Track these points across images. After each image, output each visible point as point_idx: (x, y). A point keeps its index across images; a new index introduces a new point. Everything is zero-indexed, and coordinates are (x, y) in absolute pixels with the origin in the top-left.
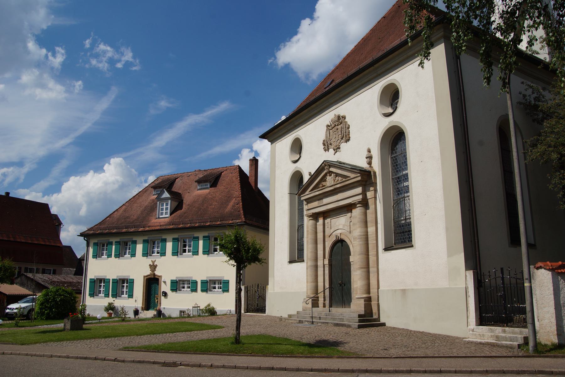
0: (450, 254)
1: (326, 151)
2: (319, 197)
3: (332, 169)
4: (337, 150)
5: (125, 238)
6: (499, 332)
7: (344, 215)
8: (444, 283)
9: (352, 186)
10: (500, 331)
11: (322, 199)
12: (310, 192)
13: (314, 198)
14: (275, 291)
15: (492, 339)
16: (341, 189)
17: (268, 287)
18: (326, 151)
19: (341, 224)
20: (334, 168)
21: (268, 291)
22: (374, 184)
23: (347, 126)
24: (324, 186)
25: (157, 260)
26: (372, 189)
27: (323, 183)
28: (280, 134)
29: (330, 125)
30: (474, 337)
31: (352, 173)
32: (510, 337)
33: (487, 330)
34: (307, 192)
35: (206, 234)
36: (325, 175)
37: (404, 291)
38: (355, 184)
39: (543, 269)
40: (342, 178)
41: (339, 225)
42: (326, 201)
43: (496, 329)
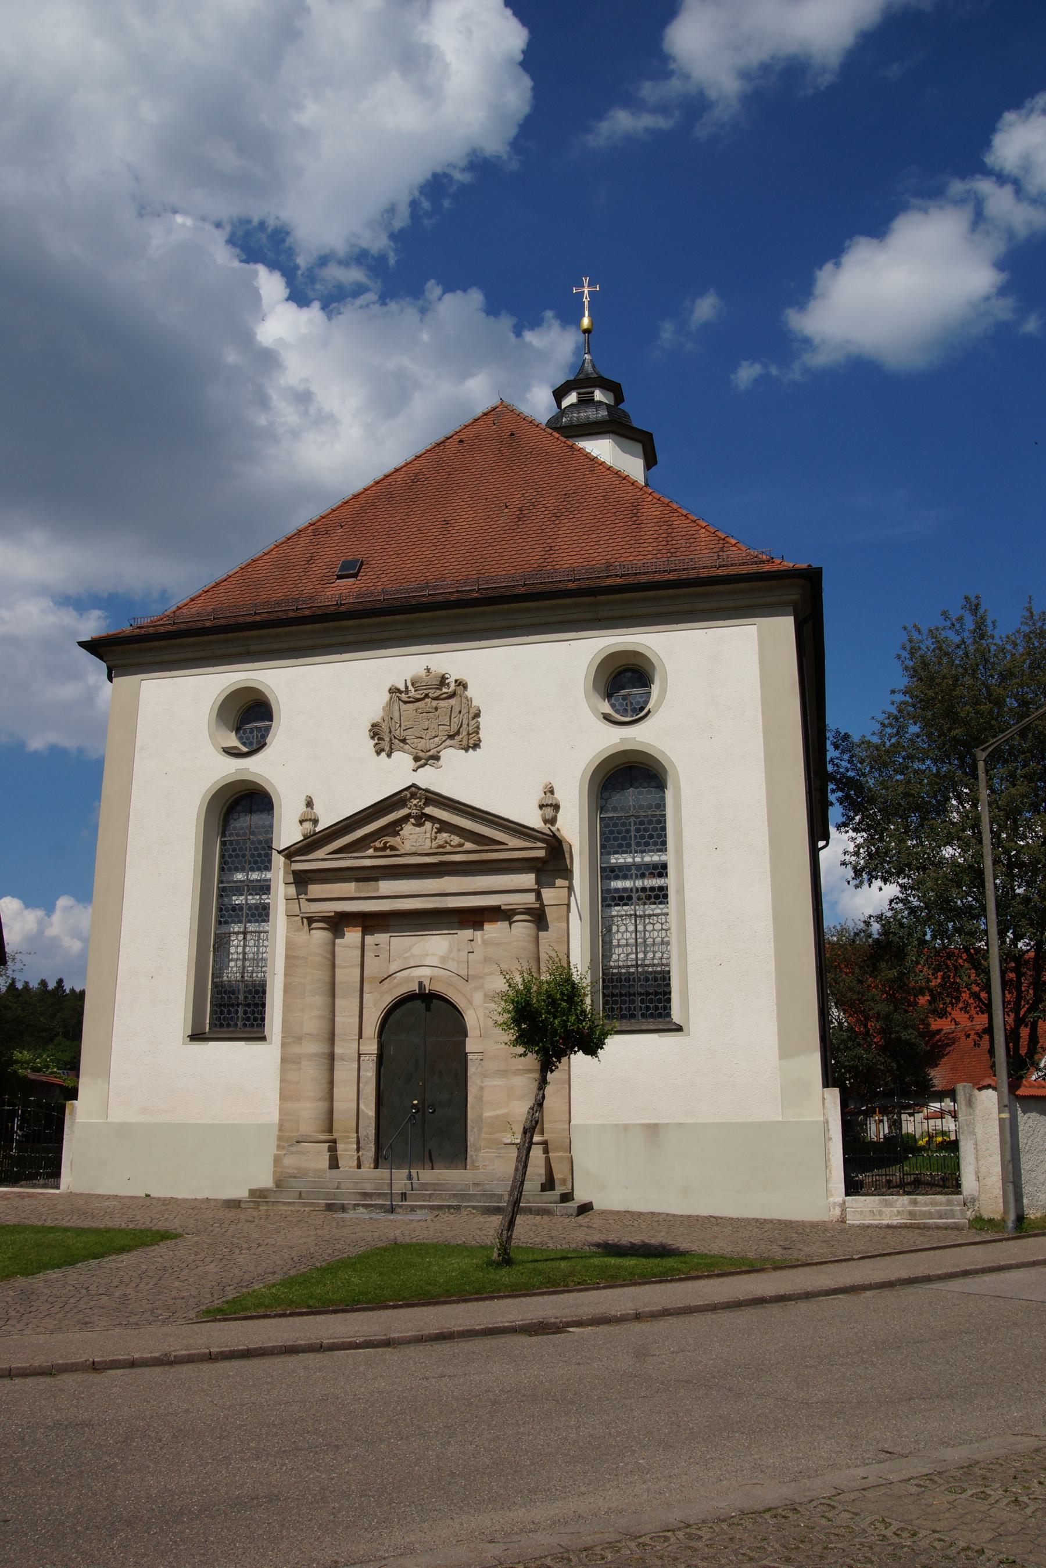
1: (378, 753)
2: (366, 874)
3: (429, 810)
4: (427, 760)
6: (903, 1204)
7: (447, 932)
8: (770, 1112)
9: (505, 865)
10: (906, 1202)
11: (376, 879)
13: (344, 873)
14: (109, 1120)
15: (899, 1217)
16: (459, 867)
17: (73, 1107)
18: (378, 753)
19: (433, 954)
20: (444, 810)
21: (73, 1120)
22: (567, 873)
23: (473, 711)
24: (393, 848)
26: (559, 882)
27: (387, 839)
29: (403, 688)
30: (858, 1217)
31: (512, 835)
32: (939, 1212)
33: (877, 1202)
34: (321, 853)
36: (405, 819)
37: (653, 1130)
39: (990, 1090)
40: (462, 841)
41: (427, 955)
42: (386, 887)
43: (897, 1200)
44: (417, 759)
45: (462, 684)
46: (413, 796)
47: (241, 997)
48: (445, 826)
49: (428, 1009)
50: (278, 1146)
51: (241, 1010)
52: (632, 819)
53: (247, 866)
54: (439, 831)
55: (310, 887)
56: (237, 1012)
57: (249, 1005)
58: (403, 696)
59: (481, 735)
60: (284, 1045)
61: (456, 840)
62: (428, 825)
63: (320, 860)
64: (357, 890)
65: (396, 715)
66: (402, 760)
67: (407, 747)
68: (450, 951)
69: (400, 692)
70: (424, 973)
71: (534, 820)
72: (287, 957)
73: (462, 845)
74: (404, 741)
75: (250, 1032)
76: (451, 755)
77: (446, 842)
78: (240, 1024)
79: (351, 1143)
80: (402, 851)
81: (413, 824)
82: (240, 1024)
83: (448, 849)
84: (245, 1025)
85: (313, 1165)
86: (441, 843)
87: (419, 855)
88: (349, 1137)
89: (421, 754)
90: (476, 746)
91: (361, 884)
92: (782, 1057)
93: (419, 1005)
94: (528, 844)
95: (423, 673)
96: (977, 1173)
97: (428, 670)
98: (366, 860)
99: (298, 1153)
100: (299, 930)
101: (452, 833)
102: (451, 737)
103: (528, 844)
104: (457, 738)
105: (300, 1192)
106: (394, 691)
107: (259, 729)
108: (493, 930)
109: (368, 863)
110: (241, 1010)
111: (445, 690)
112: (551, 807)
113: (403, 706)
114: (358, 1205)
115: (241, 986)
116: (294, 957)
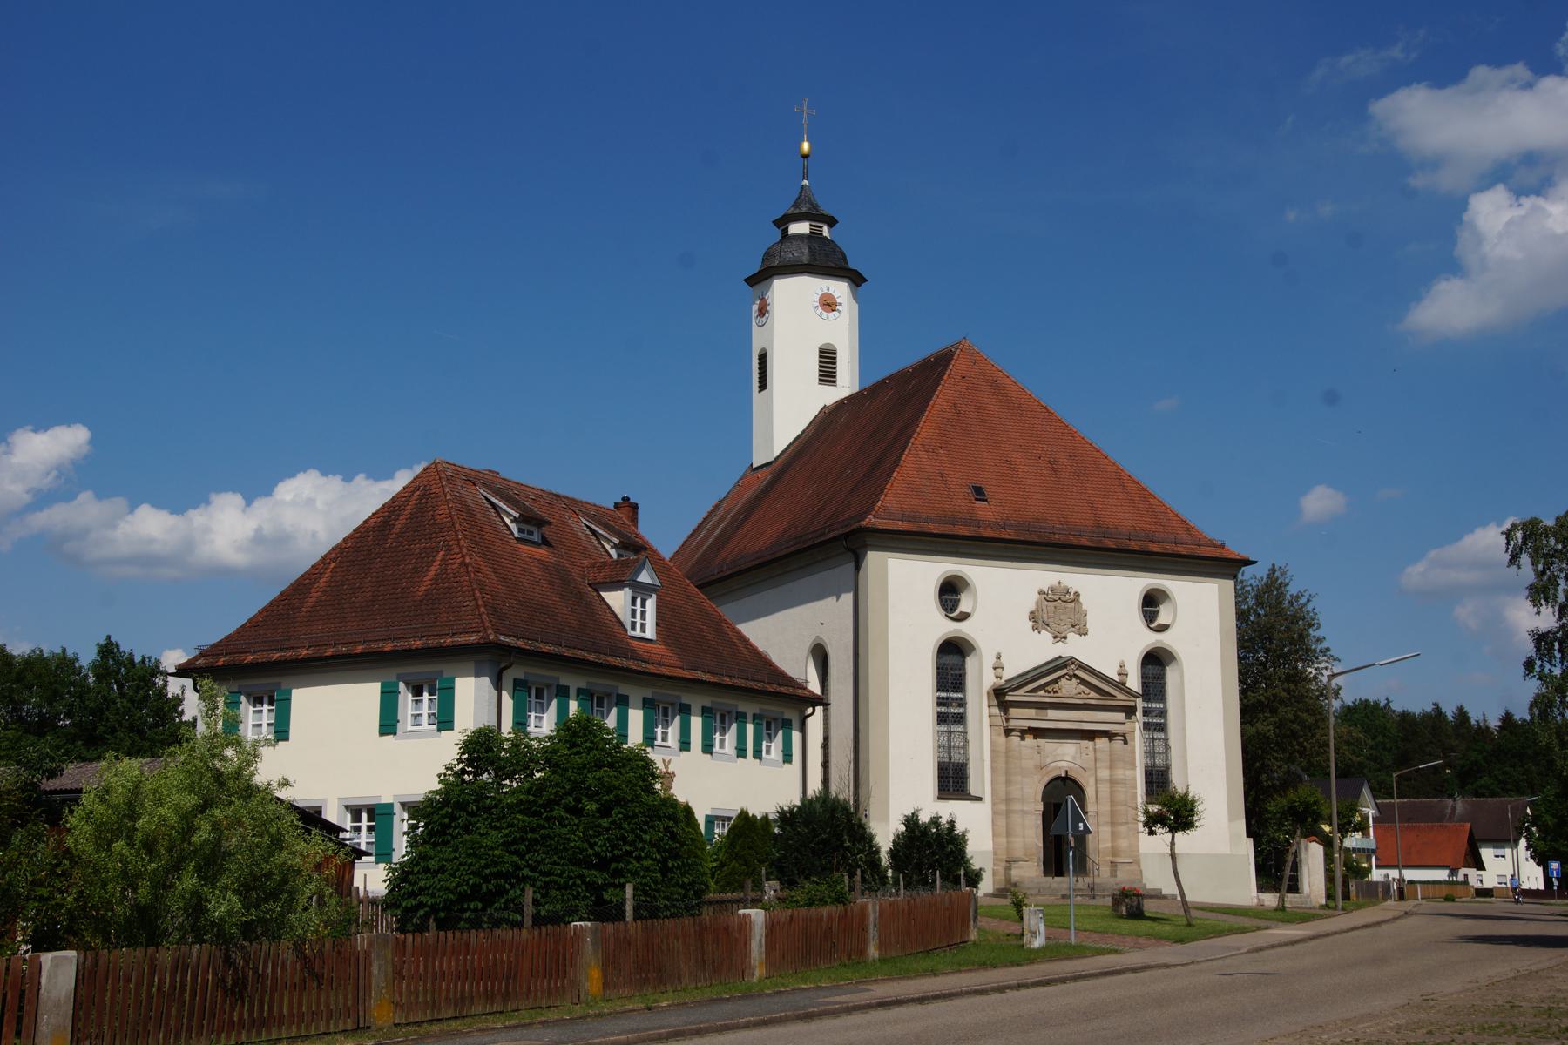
3: (1077, 672)
5: (727, 701)
8: (1224, 849)
11: (1046, 709)
12: (1028, 692)
24: (1056, 692)
25: (674, 758)
28: (912, 547)
34: (1021, 691)
35: (648, 693)
38: (1119, 708)
42: (1052, 714)
44: (1055, 637)
46: (1073, 663)
47: (951, 772)
48: (1083, 682)
49: (1065, 785)
50: (994, 865)
51: (951, 781)
54: (1078, 684)
55: (1011, 709)
56: (948, 782)
59: (1088, 626)
60: (994, 804)
61: (1087, 690)
62: (1074, 680)
64: (1037, 714)
65: (1044, 608)
66: (1046, 636)
68: (1076, 753)
69: (1045, 593)
70: (1064, 764)
71: (1116, 678)
72: (993, 751)
74: (1048, 625)
76: (1072, 636)
78: (951, 789)
80: (1060, 695)
82: (951, 789)
83: (1083, 695)
84: (954, 790)
85: (1027, 875)
90: (1086, 634)
94: (1126, 698)
95: (1057, 584)
96: (1309, 883)
97: (1059, 583)
98: (1041, 696)
100: (1000, 735)
101: (1085, 686)
102: (1073, 626)
103: (1126, 698)
106: (1041, 592)
107: (951, 600)
108: (1102, 743)
109: (1047, 700)
110: (951, 781)
111: (1068, 596)
114: (1077, 895)
115: (951, 765)
116: (998, 752)
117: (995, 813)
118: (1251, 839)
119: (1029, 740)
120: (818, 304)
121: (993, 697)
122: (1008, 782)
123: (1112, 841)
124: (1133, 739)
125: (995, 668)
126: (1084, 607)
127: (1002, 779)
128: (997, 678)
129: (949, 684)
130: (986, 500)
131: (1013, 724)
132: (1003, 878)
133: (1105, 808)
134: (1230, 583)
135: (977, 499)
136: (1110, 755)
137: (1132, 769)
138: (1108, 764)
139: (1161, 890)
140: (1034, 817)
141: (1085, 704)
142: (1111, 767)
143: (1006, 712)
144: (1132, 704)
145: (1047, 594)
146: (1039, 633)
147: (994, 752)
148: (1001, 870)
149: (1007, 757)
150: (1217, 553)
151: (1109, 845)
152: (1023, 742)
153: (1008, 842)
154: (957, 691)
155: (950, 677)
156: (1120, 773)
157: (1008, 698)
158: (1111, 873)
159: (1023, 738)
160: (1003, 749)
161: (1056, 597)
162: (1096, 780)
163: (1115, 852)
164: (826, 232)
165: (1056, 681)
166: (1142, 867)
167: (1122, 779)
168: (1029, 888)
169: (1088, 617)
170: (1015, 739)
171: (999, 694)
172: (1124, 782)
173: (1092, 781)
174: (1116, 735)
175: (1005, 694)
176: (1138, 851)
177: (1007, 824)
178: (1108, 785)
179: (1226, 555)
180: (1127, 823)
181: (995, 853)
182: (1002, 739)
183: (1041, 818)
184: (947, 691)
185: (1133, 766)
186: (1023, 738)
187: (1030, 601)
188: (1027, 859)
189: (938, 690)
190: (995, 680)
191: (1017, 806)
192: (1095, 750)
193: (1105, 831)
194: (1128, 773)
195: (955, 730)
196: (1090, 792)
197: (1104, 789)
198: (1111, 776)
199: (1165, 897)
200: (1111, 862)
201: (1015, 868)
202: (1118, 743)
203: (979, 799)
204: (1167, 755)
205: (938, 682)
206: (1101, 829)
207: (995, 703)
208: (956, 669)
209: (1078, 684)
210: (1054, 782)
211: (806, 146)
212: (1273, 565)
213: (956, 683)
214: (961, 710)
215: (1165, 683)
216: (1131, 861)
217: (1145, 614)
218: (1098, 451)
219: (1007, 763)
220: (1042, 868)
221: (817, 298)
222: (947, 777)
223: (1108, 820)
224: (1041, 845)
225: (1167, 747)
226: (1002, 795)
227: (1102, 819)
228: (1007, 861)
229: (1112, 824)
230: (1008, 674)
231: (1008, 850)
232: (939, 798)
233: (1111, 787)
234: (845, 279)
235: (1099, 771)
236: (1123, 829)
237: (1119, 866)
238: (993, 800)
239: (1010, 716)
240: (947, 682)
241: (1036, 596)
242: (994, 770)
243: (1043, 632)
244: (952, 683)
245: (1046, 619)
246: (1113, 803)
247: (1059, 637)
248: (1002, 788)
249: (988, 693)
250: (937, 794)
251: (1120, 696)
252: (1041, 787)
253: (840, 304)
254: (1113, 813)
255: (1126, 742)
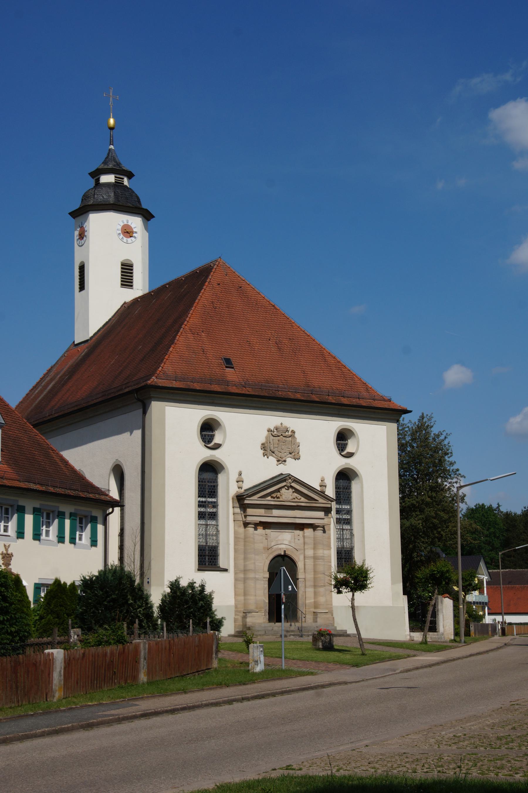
0: (393, 582)
1: (264, 456)
2: (268, 507)
3: (293, 484)
5: (51, 504)
8: (388, 603)
11: (272, 509)
13: (262, 506)
18: (264, 456)
24: (278, 498)
25: (13, 544)
34: (255, 497)
38: (320, 509)
42: (276, 512)
44: (278, 461)
45: (293, 432)
46: (290, 478)
47: (207, 552)
48: (297, 491)
49: (283, 560)
50: (236, 615)
51: (207, 558)
52: (342, 493)
53: (207, 496)
54: (293, 492)
55: (248, 510)
56: (205, 559)
57: (211, 556)
58: (273, 434)
59: (300, 453)
60: (236, 573)
61: (299, 497)
62: (290, 489)
63: (254, 500)
64: (265, 513)
65: (271, 441)
66: (272, 460)
67: (274, 455)
68: (292, 539)
69: (271, 431)
70: (283, 546)
73: (300, 499)
74: (273, 452)
75: (211, 567)
76: (290, 461)
77: (296, 497)
79: (262, 613)
80: (281, 499)
81: (286, 489)
82: (207, 564)
83: (296, 500)
84: (209, 564)
86: (295, 497)
87: (289, 501)
88: (261, 610)
89: (280, 459)
90: (299, 459)
91: (266, 510)
92: (392, 584)
93: (280, 559)
96: (443, 625)
97: (282, 424)
98: (269, 501)
99: (252, 617)
102: (290, 453)
104: (293, 454)
105: (265, 632)
106: (269, 430)
107: (208, 435)
108: (308, 532)
109: (273, 503)
110: (207, 558)
111: (287, 433)
112: (323, 486)
113: (273, 437)
114: (291, 635)
115: (207, 548)
116: (239, 538)
117: (236, 580)
118: (406, 596)
119: (260, 530)
120: (120, 232)
121: (236, 501)
122: (245, 559)
123: (315, 598)
124: (329, 530)
125: (237, 482)
126: (298, 441)
127: (242, 556)
128: (239, 488)
129: (207, 492)
130: (233, 368)
131: (249, 519)
132: (242, 624)
133: (310, 576)
134: (394, 426)
135: (227, 367)
136: (314, 540)
137: (329, 550)
138: (312, 546)
139: (346, 630)
140: (262, 582)
141: (297, 506)
142: (315, 548)
143: (245, 511)
144: (329, 506)
145: (274, 432)
146: (268, 458)
147: (236, 538)
148: (239, 618)
149: (245, 542)
150: (385, 405)
151: (313, 600)
152: (256, 532)
153: (245, 599)
154: (212, 497)
155: (207, 487)
156: (320, 552)
157: (246, 502)
158: (314, 620)
159: (256, 529)
160: (242, 536)
161: (279, 434)
162: (304, 557)
163: (316, 605)
164: (126, 182)
165: (278, 490)
166: (334, 615)
167: (321, 556)
168: (258, 631)
169: (300, 447)
170: (250, 529)
171: (240, 499)
172: (322, 558)
173: (302, 557)
174: (318, 526)
175: (244, 499)
176: (332, 605)
177: (245, 588)
178: (312, 560)
179: (392, 407)
180: (324, 586)
181: (236, 607)
182: (242, 529)
183: (267, 582)
184: (205, 497)
185: (329, 548)
186: (256, 529)
187: (262, 436)
188: (257, 611)
189: (199, 497)
190: (238, 490)
191: (251, 575)
192: (304, 537)
193: (310, 591)
194: (326, 552)
195: (210, 523)
196: (300, 565)
197: (310, 563)
198: (314, 554)
199: (349, 636)
200: (314, 613)
201: (250, 617)
202: (319, 532)
203: (226, 570)
204: (351, 541)
205: (199, 491)
206: (307, 590)
207: (237, 505)
208: (211, 482)
209: (293, 492)
210: (276, 559)
211: (112, 121)
212: (423, 414)
213: (211, 492)
214: (214, 510)
215: (351, 492)
216: (327, 611)
217: (338, 445)
218: (309, 336)
219: (245, 545)
220: (267, 617)
221: (120, 228)
222: (204, 556)
223: (312, 584)
224: (267, 601)
225: (352, 535)
226: (242, 568)
227: (308, 583)
228: (244, 612)
229: (315, 586)
230: (247, 485)
231: (245, 604)
232: (199, 570)
233: (314, 562)
234: (140, 216)
235: (306, 551)
236: (322, 590)
237: (319, 615)
238: (235, 571)
239: (247, 514)
240: (205, 491)
241: (266, 433)
242: (236, 551)
243: (270, 457)
244: (209, 492)
245: (272, 448)
246: (315, 572)
247: (281, 461)
248: (241, 562)
249: (233, 499)
250: (197, 568)
251: (321, 500)
252: (268, 562)
253: (136, 233)
254: (315, 579)
255: (324, 532)
